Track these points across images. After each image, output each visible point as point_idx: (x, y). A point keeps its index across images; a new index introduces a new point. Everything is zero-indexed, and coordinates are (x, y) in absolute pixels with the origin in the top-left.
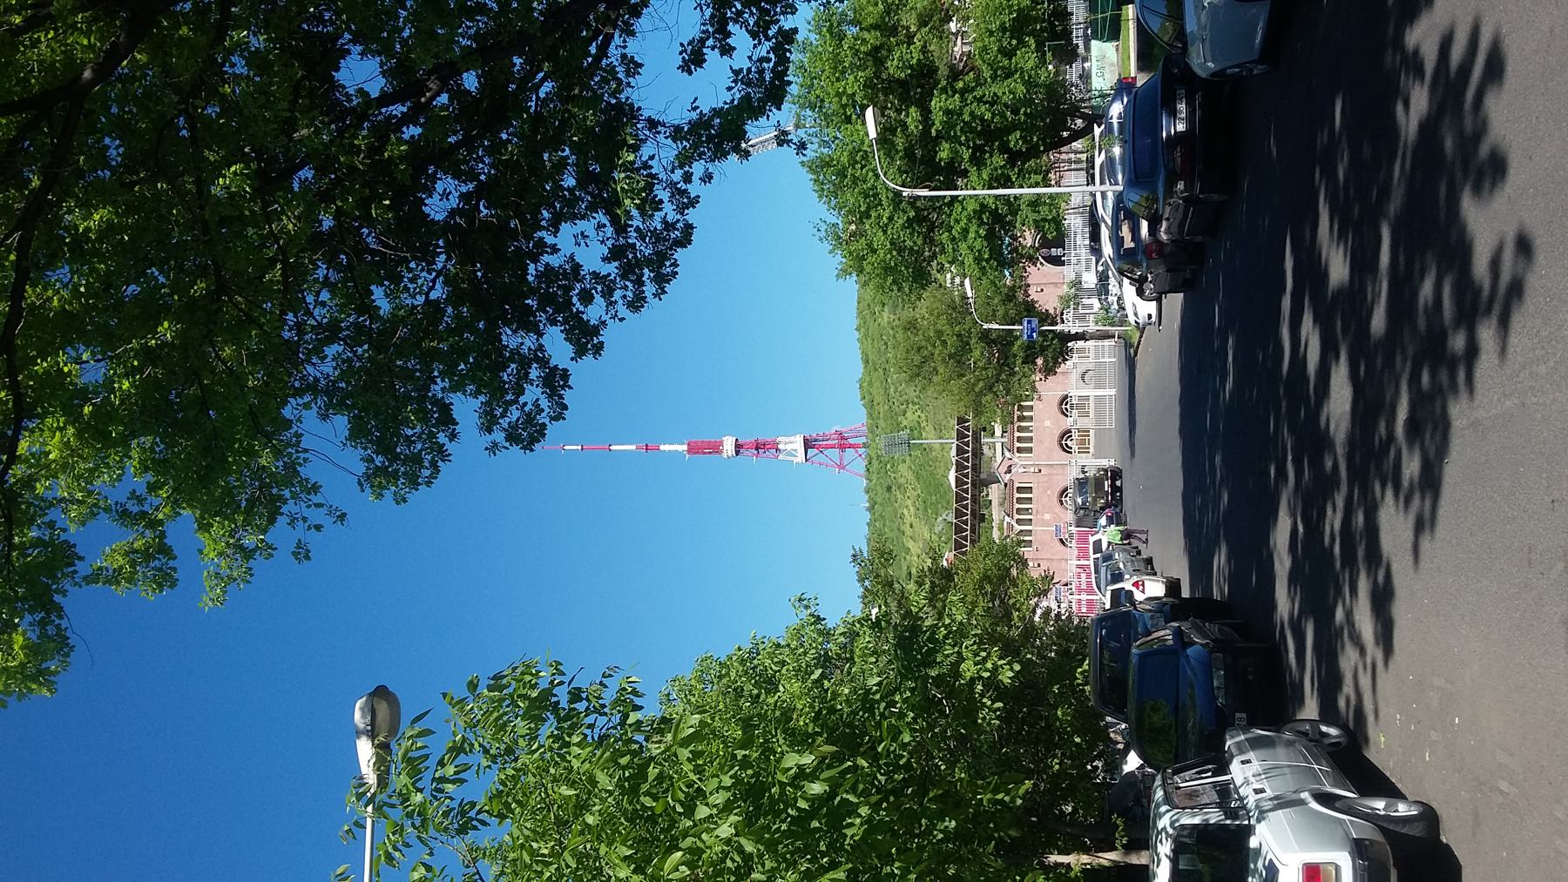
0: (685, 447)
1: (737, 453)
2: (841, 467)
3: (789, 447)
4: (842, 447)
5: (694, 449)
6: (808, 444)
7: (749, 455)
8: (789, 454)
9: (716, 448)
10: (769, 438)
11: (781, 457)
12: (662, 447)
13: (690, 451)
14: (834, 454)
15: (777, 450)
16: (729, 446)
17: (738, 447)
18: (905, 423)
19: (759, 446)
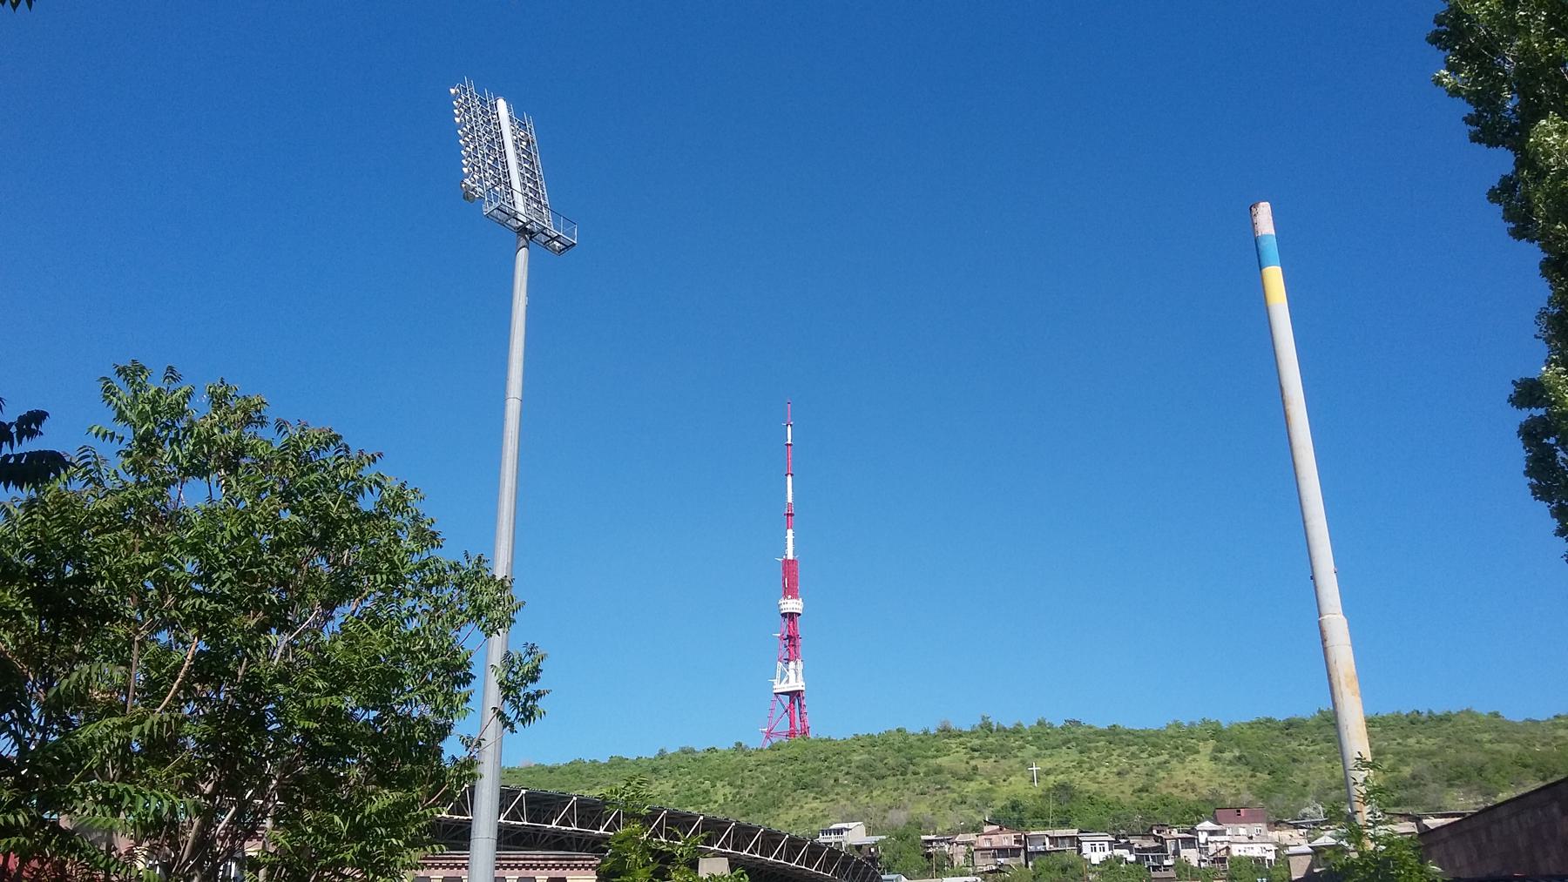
0: (790, 557)
1: (784, 615)
2: (769, 734)
3: (791, 674)
4: (792, 734)
5: (789, 566)
6: (795, 695)
7: (780, 629)
8: (783, 674)
9: (790, 591)
10: (801, 651)
11: (780, 665)
12: (790, 532)
13: (786, 561)
16: (792, 605)
17: (791, 616)
18: (719, 784)
19: (792, 639)
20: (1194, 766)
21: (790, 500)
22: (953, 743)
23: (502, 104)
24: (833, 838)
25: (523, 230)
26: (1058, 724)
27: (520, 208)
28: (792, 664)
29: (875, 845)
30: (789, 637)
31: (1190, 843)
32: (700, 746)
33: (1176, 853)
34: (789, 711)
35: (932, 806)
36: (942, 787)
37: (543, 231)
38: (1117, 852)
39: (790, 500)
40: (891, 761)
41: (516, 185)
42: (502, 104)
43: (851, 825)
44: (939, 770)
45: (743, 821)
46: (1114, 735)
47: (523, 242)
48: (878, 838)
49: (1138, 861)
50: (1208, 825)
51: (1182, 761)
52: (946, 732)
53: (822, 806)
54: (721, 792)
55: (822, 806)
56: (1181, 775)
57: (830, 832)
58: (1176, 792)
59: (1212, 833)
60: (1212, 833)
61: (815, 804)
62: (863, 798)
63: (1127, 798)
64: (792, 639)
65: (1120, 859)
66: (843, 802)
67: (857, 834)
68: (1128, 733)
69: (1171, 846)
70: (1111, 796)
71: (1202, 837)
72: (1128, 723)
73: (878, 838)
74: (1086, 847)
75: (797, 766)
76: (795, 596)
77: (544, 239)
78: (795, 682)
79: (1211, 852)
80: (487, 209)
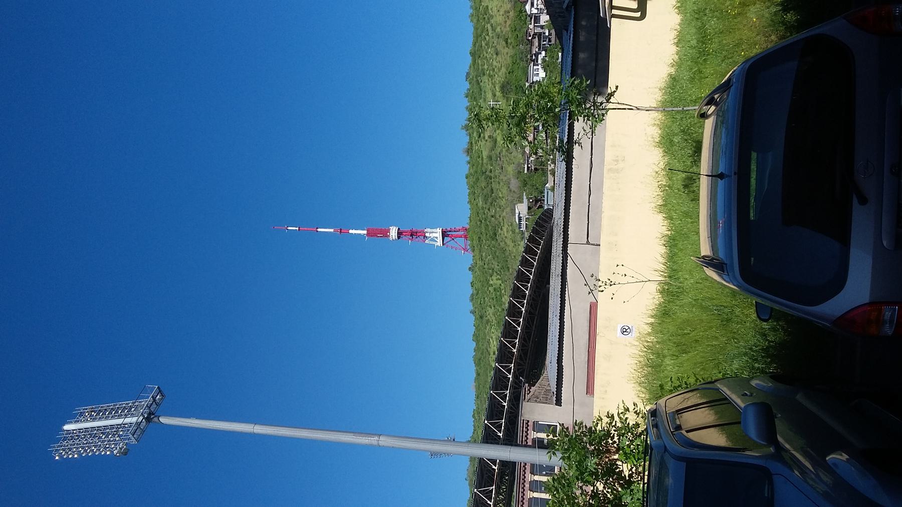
0: (365, 232)
1: (399, 237)
4: (466, 237)
6: (444, 234)
7: (407, 241)
8: (433, 240)
9: (385, 233)
10: (419, 229)
11: (427, 241)
12: (351, 231)
13: (368, 234)
14: (461, 241)
15: (425, 236)
16: (393, 233)
17: (400, 234)
19: (413, 234)
20: (495, 9)
21: (332, 230)
22: (475, 148)
23: (66, 427)
24: (523, 223)
25: (148, 419)
26: (467, 85)
27: (134, 420)
28: (427, 235)
29: (528, 199)
30: (412, 235)
31: (537, 19)
32: (470, 291)
33: (542, 27)
34: (453, 238)
35: (509, 164)
36: (499, 156)
37: (149, 407)
38: (540, 62)
39: (332, 230)
40: (483, 184)
41: (120, 421)
42: (66, 427)
43: (517, 211)
44: (490, 158)
45: (510, 292)
46: (475, 54)
47: (156, 419)
48: (525, 197)
49: (546, 51)
50: (528, 7)
51: (492, 17)
52: (469, 151)
53: (506, 226)
54: (495, 281)
55: (506, 226)
56: (499, 19)
57: (520, 224)
58: (508, 23)
59: (532, 5)
60: (532, 5)
61: (505, 229)
62: (503, 202)
63: (511, 51)
64: (413, 234)
65: (543, 59)
66: (504, 214)
67: (522, 209)
68: (474, 45)
69: (538, 30)
70: (509, 61)
71: (534, 11)
72: (469, 46)
73: (525, 197)
74: (535, 79)
75: (483, 238)
76: (388, 231)
77: (154, 406)
78: (437, 234)
79: (542, 7)
80: (133, 441)
